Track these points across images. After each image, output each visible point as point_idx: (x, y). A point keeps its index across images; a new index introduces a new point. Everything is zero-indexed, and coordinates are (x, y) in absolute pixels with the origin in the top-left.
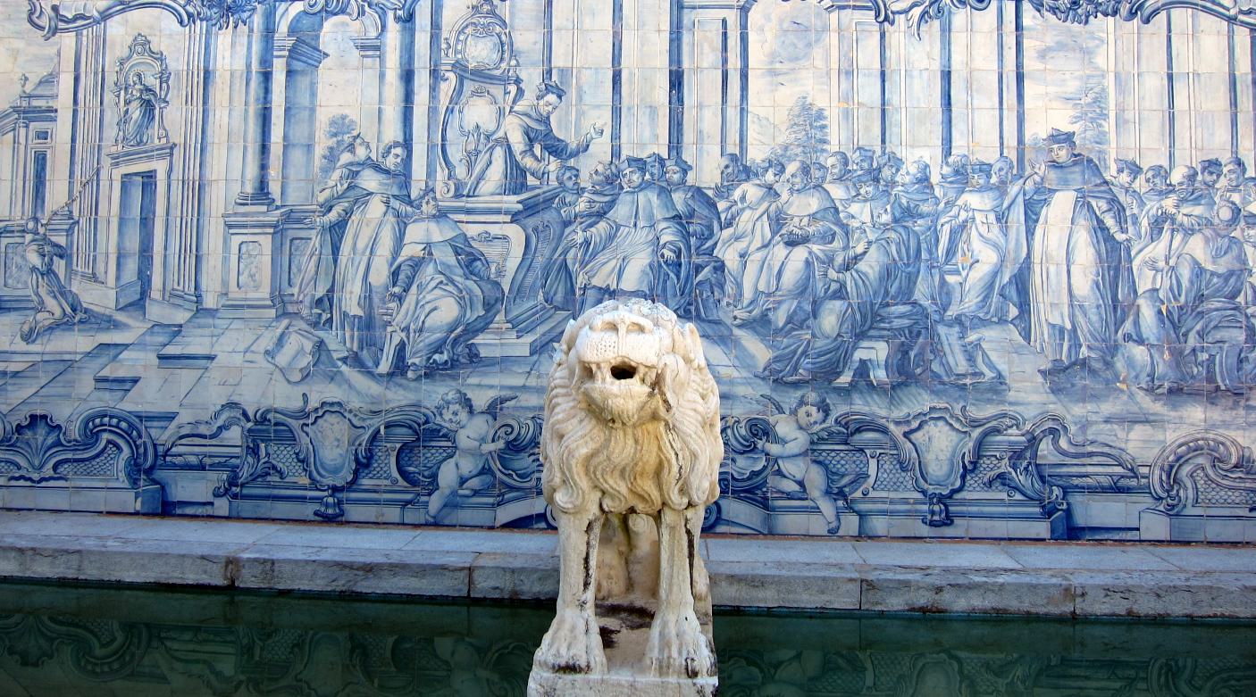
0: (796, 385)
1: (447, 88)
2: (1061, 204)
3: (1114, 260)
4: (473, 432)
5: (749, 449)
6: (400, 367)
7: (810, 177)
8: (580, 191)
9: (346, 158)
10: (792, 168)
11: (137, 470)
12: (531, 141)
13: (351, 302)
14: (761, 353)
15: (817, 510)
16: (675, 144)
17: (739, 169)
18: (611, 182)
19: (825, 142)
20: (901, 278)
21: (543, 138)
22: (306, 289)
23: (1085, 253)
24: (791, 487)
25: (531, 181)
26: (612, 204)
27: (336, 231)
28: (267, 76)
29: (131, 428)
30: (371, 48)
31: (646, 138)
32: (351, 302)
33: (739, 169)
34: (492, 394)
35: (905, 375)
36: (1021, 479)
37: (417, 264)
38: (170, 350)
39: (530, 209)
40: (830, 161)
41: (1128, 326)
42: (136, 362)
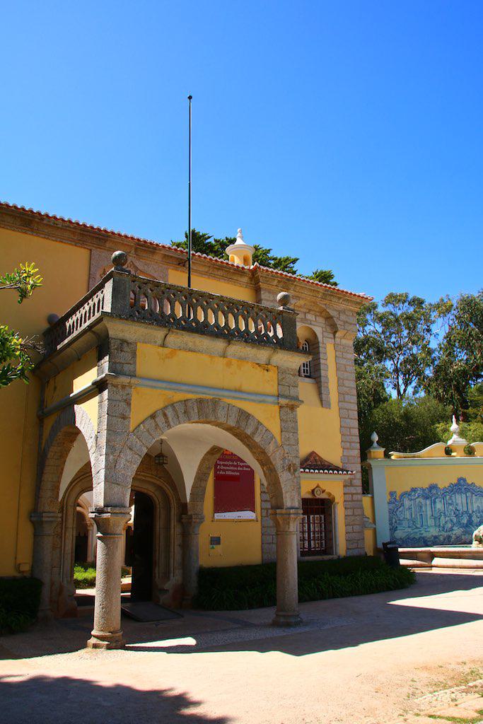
7: (479, 513)
11: (424, 542)
17: (473, 512)
29: (423, 538)
30: (440, 501)
31: (465, 509)
32: (441, 525)
33: (473, 512)
42: (422, 532)
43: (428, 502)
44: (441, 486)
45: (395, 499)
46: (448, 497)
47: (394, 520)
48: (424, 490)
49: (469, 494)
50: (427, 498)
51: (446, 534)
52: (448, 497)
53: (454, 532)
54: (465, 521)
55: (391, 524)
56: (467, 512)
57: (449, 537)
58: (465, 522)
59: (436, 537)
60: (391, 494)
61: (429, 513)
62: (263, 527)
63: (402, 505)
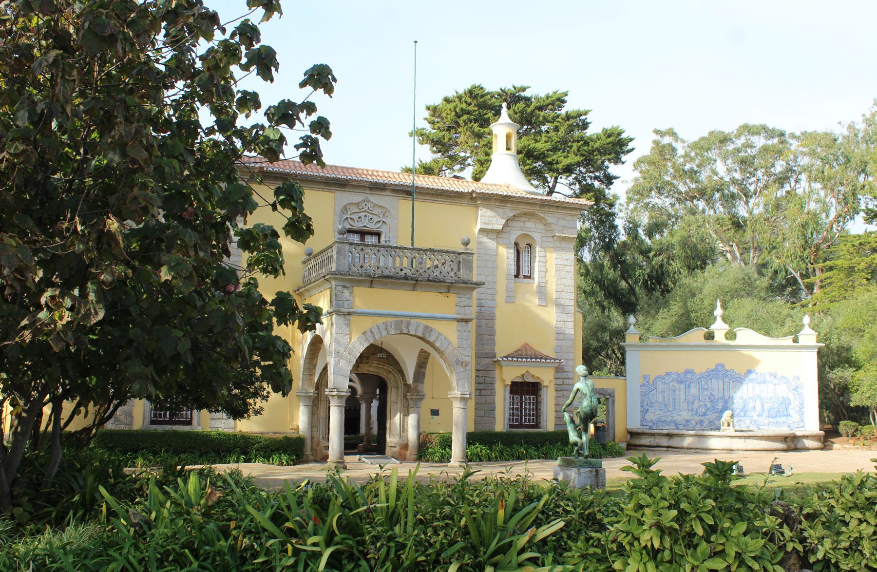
2: (758, 401)
3: (763, 405)
4: (706, 421)
13: (695, 409)
18: (718, 399)
20: (744, 407)
22: (690, 409)
23: (760, 405)
29: (675, 421)
31: (721, 395)
32: (695, 409)
35: (745, 415)
42: (674, 415)
43: (682, 386)
45: (648, 382)
46: (703, 382)
47: (645, 403)
48: (678, 375)
49: (726, 380)
50: (681, 382)
51: (697, 418)
52: (703, 382)
53: (707, 417)
56: (723, 398)
57: (702, 421)
58: (720, 407)
59: (687, 421)
60: (645, 377)
61: (683, 397)
62: (476, 404)
63: (655, 388)
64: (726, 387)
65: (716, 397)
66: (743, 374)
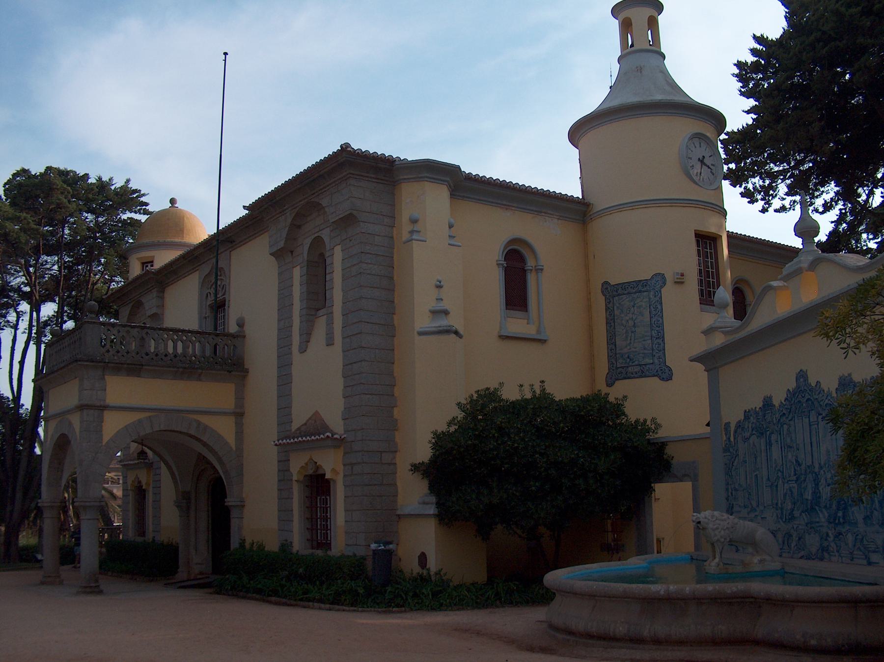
0: (831, 523)
1: (786, 450)
5: (826, 540)
6: (786, 519)
8: (802, 474)
9: (777, 469)
10: (827, 466)
12: (796, 462)
14: (827, 515)
15: (835, 556)
16: (813, 462)
18: (806, 471)
19: (830, 458)
21: (797, 461)
24: (832, 549)
25: (797, 473)
26: (806, 477)
27: (777, 486)
28: (767, 450)
33: (821, 467)
34: (797, 526)
36: (862, 548)
37: (786, 494)
38: (762, 516)
39: (797, 479)
40: (831, 463)
41: (874, 506)
44: (776, 402)
47: (730, 490)
48: (757, 413)
54: (808, 496)
55: (727, 499)
58: (810, 498)
64: (814, 440)
65: (803, 466)
66: (834, 395)
